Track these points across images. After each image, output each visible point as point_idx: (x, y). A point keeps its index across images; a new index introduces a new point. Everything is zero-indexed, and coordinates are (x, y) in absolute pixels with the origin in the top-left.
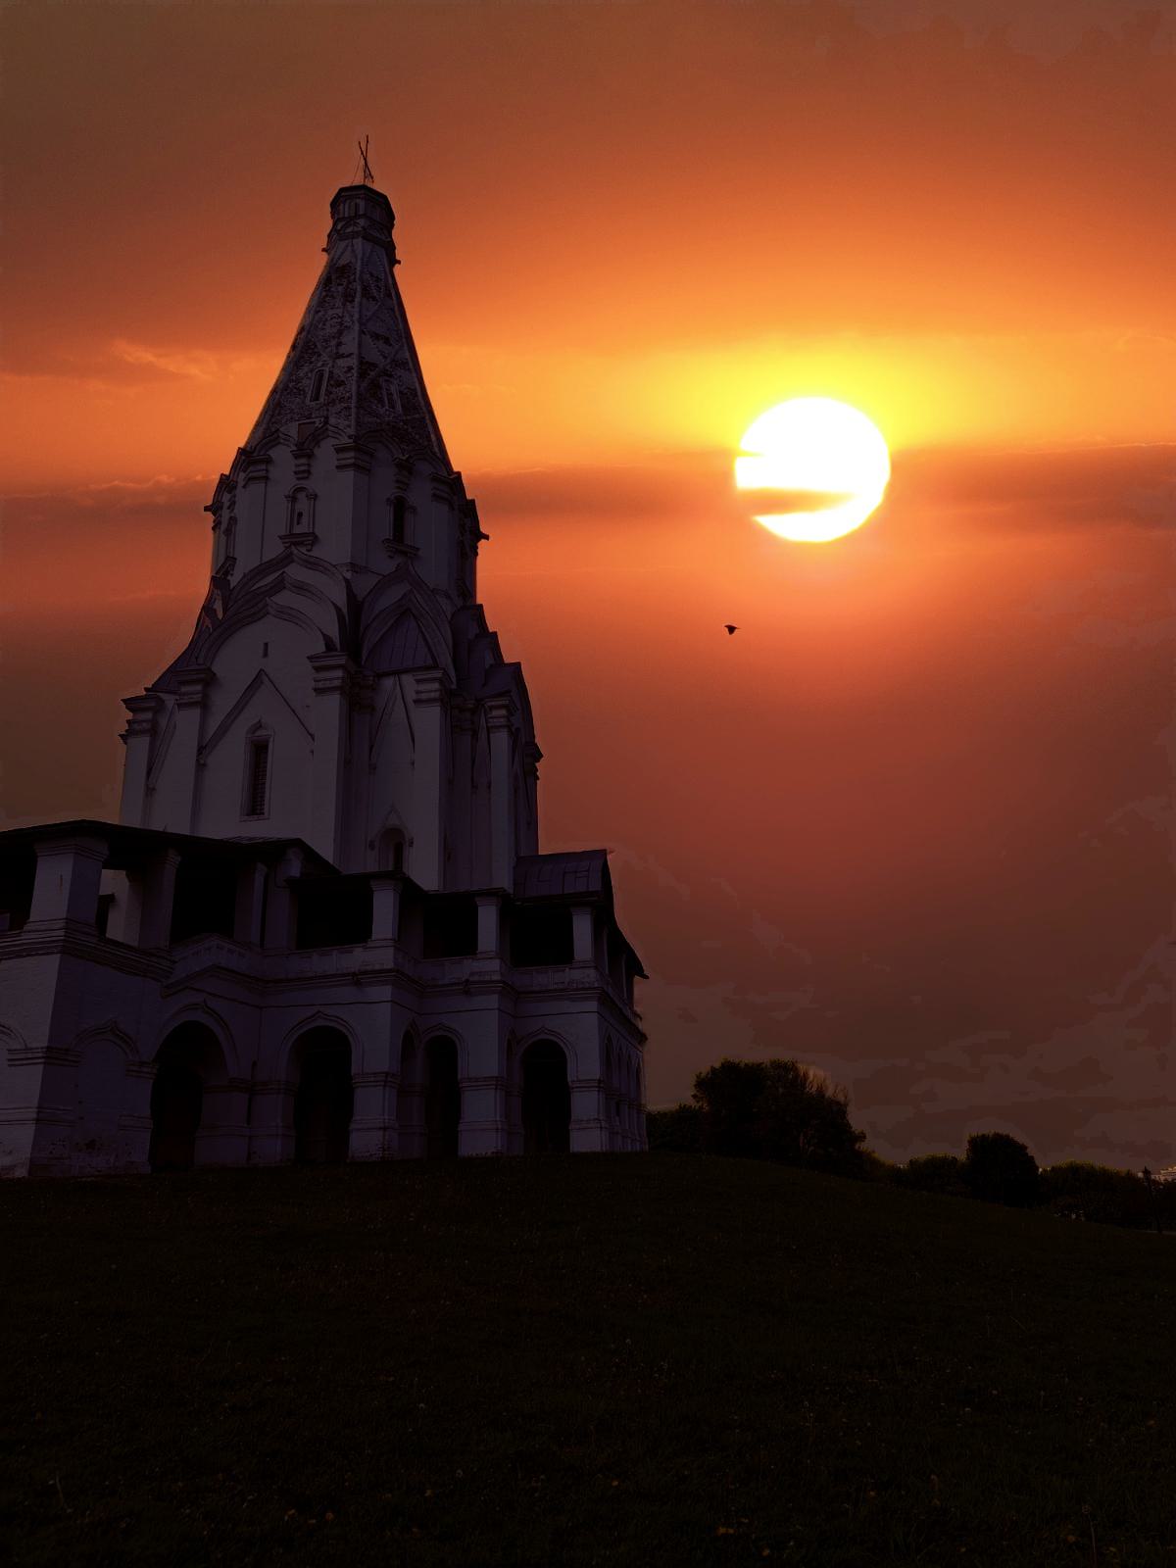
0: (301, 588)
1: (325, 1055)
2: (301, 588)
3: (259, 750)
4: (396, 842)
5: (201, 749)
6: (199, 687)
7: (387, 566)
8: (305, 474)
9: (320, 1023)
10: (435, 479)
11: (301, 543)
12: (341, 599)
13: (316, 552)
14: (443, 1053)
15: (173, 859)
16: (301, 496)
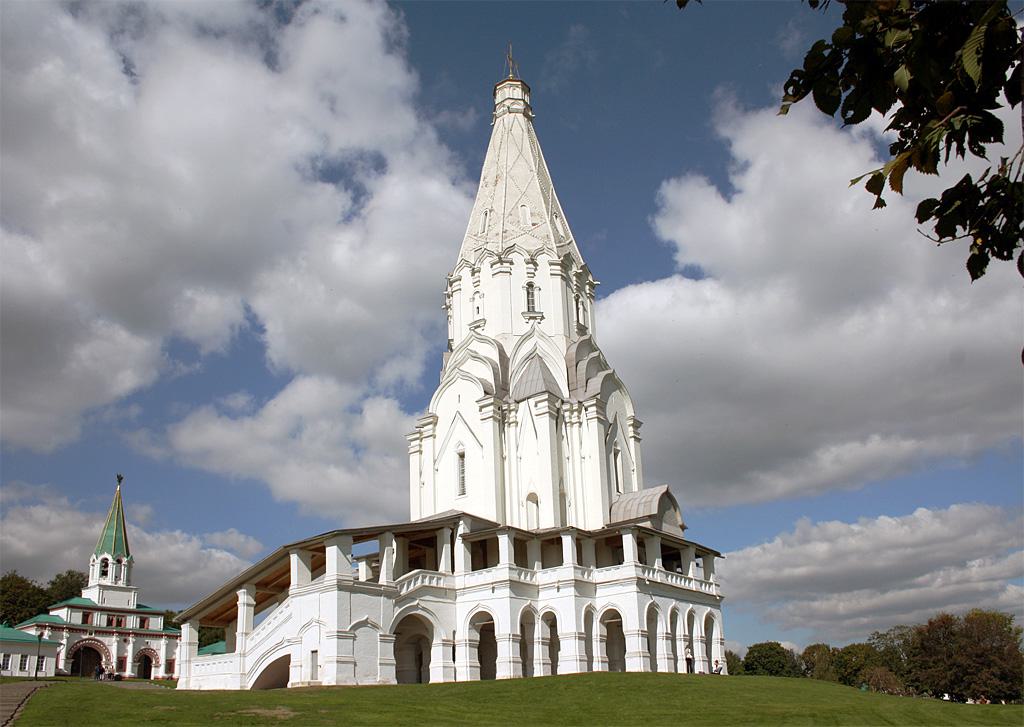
0: (476, 357)
1: (484, 627)
2: (476, 357)
3: (462, 456)
4: (533, 498)
5: (435, 462)
6: (431, 426)
7: (524, 327)
8: (477, 284)
9: (480, 609)
10: (551, 264)
11: (479, 327)
12: (496, 358)
16: (477, 295)
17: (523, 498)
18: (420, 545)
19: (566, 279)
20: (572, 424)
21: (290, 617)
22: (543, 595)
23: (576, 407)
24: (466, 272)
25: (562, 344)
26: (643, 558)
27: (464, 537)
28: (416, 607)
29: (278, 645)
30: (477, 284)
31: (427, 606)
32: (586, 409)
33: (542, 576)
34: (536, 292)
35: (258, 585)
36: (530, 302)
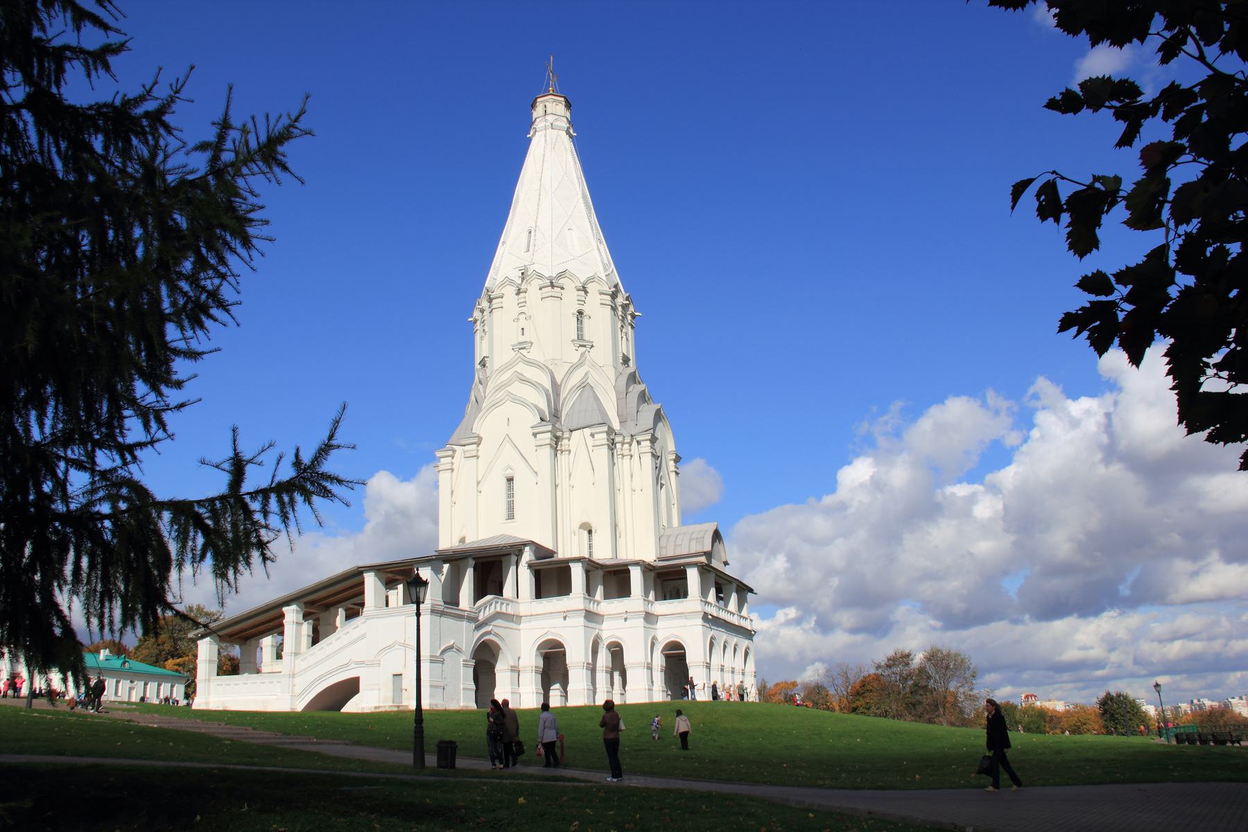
3: (510, 480)
5: (478, 483)
7: (575, 356)
8: (522, 304)
12: (548, 386)
13: (533, 354)
14: (617, 652)
15: (472, 562)
17: (576, 525)
18: (489, 568)
19: (614, 309)
20: (623, 456)
21: (363, 637)
22: (606, 625)
23: (628, 440)
24: (510, 291)
25: (612, 374)
26: (704, 593)
27: (530, 566)
28: (489, 633)
29: (342, 667)
30: (522, 304)
31: (498, 632)
32: (639, 443)
33: (609, 607)
34: (585, 321)
35: (307, 604)
36: (580, 329)
